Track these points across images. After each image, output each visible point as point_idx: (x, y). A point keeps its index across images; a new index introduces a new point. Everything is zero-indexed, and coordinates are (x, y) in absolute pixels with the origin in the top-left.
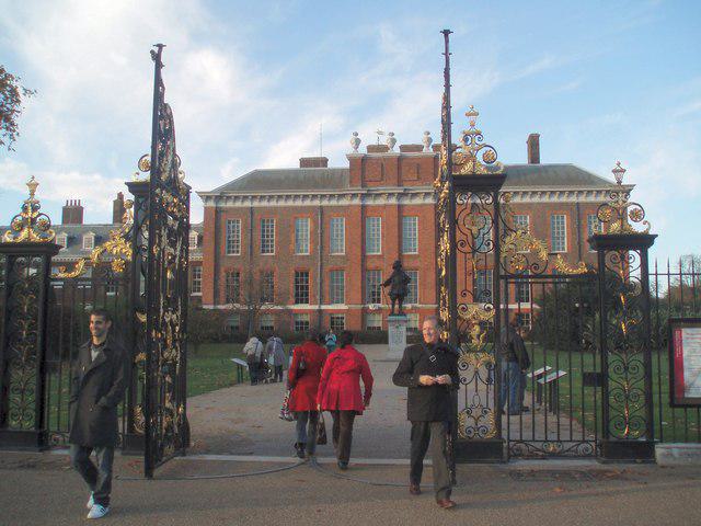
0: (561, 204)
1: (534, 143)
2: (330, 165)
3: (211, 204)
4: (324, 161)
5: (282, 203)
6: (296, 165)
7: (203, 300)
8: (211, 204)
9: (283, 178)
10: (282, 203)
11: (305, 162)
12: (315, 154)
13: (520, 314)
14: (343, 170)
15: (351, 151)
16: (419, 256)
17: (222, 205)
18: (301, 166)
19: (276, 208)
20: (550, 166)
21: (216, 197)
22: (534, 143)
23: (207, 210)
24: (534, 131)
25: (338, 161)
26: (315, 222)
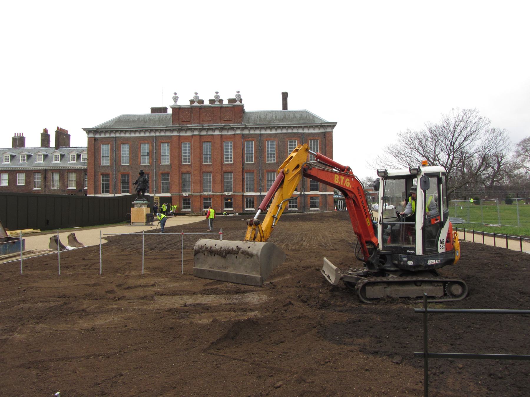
0: (295, 133)
3: (91, 135)
5: (133, 135)
6: (149, 112)
7: (88, 191)
8: (91, 135)
10: (133, 135)
15: (172, 103)
16: (212, 165)
17: (98, 136)
20: (292, 111)
21: (94, 131)
23: (89, 138)
24: (284, 91)
26: (152, 146)
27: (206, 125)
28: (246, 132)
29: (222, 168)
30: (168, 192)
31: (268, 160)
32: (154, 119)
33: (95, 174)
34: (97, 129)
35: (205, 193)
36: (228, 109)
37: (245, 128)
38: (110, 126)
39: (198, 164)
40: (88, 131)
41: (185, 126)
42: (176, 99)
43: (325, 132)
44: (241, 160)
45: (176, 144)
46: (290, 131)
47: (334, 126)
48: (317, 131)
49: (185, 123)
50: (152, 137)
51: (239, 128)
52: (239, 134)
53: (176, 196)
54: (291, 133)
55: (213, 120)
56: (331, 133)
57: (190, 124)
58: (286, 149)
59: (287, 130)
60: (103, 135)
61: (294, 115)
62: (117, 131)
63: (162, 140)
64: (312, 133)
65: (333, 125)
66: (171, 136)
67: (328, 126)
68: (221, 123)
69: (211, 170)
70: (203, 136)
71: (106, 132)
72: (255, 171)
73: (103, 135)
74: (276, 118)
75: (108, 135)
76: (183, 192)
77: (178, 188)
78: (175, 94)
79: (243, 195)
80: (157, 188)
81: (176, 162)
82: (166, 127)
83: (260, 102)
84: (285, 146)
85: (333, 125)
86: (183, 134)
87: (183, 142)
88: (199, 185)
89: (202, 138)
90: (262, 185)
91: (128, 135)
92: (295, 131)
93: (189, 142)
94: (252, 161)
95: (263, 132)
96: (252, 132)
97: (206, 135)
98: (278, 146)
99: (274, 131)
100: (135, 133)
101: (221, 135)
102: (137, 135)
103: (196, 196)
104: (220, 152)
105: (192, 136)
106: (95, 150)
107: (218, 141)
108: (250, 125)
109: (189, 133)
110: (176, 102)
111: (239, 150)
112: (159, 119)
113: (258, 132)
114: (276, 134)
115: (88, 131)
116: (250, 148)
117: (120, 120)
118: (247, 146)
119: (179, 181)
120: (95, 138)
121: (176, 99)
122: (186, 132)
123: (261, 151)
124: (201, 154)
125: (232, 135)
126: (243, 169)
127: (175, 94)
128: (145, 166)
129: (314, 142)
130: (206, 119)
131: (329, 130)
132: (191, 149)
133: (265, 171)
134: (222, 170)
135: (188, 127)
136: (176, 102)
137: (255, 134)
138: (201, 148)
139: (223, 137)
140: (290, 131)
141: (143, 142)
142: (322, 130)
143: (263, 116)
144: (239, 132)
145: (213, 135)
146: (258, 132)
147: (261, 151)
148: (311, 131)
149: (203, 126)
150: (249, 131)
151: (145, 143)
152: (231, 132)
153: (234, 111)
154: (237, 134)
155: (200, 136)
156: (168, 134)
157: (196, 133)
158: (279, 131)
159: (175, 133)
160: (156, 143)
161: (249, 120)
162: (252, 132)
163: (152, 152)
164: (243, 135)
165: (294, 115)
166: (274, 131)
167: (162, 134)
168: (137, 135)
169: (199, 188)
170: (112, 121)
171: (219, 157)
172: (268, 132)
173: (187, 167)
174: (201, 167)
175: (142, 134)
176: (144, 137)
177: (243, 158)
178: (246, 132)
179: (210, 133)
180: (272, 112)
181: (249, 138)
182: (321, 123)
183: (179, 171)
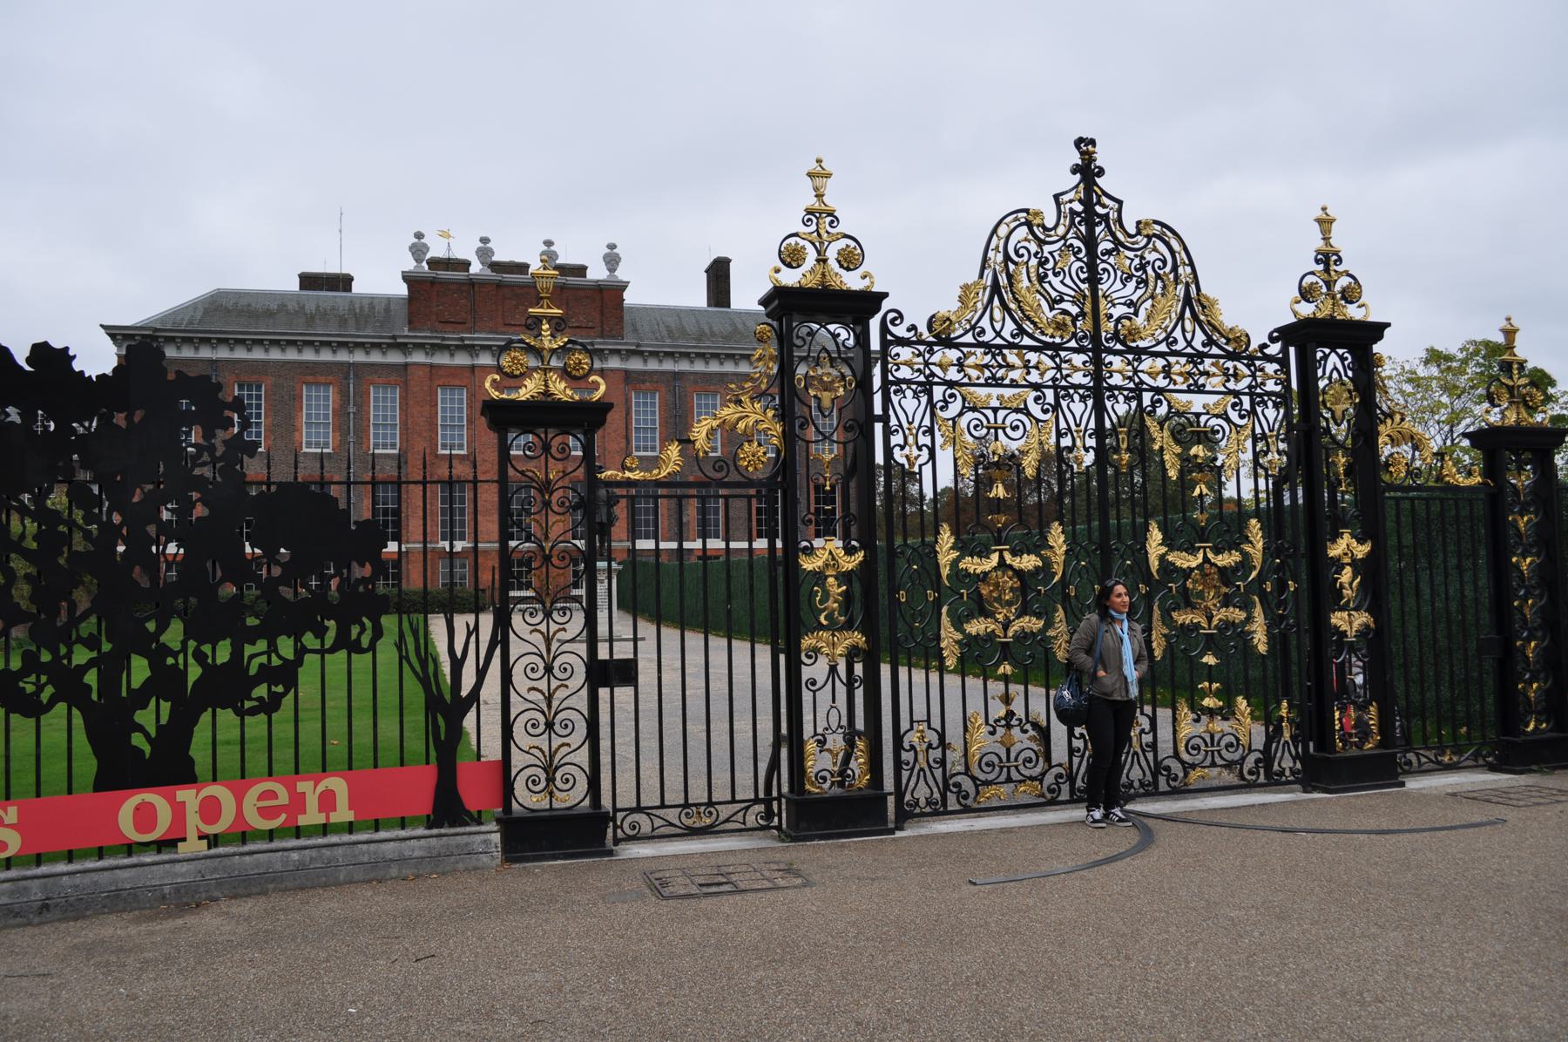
2: (357, 288)
5: (275, 355)
9: (274, 306)
12: (333, 268)
13: (705, 554)
14: (389, 300)
15: (410, 264)
18: (302, 287)
19: (265, 363)
25: (381, 277)
26: (344, 394)
28: (635, 364)
32: (333, 309)
34: (156, 330)
38: (191, 323)
41: (452, 337)
42: (418, 250)
44: (623, 445)
49: (449, 327)
50: (342, 364)
51: (618, 352)
66: (406, 365)
78: (419, 236)
82: (394, 337)
86: (442, 359)
87: (443, 386)
91: (258, 354)
95: (684, 366)
96: (653, 365)
112: (352, 310)
113: (668, 366)
118: (638, 404)
122: (452, 355)
127: (419, 236)
135: (462, 339)
136: (419, 261)
141: (310, 379)
143: (672, 322)
146: (668, 366)
150: (645, 361)
156: (395, 358)
161: (635, 330)
162: (653, 365)
163: (341, 413)
164: (626, 372)
167: (376, 357)
168: (292, 355)
170: (194, 306)
172: (699, 366)
175: (308, 355)
176: (315, 363)
177: (628, 439)
178: (635, 364)
180: (693, 312)
181: (643, 382)
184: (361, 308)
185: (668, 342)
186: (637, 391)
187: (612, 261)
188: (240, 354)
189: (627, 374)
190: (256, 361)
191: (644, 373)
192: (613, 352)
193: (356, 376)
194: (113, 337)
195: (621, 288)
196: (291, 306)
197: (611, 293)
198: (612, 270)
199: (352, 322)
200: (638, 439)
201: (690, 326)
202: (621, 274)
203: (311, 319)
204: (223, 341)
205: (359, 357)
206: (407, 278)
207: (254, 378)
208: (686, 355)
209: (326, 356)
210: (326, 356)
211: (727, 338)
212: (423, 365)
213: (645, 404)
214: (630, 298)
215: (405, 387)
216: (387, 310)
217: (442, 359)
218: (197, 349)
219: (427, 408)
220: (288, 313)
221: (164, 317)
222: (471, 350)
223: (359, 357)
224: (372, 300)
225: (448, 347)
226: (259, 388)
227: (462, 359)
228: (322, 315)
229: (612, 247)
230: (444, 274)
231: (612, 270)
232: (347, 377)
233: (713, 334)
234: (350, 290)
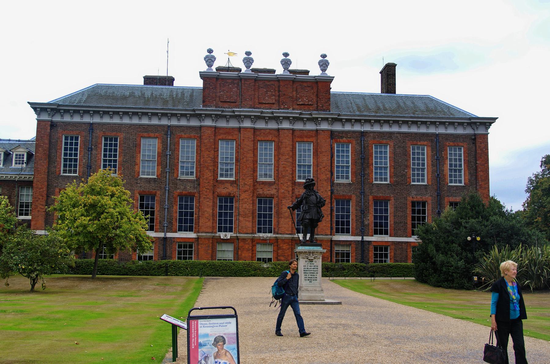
0: (423, 134)
1: (389, 74)
2: (176, 84)
3: (45, 117)
4: (170, 81)
5: (126, 120)
6: (141, 82)
7: (32, 223)
8: (45, 117)
11: (149, 80)
12: (162, 73)
14: (193, 90)
15: (204, 68)
16: (274, 183)
17: (57, 118)
18: (145, 83)
19: (120, 125)
20: (407, 97)
21: (52, 109)
22: (389, 74)
23: (39, 122)
25: (189, 78)
27: (267, 112)
28: (337, 127)
29: (293, 189)
30: (191, 230)
31: (376, 179)
33: (48, 191)
34: (59, 105)
35: (261, 235)
36: (305, 84)
37: (335, 120)
38: (80, 102)
39: (250, 181)
40: (38, 108)
41: (228, 111)
42: (210, 60)
43: (475, 135)
44: (329, 175)
45: (208, 141)
46: (414, 129)
47: (490, 124)
48: (460, 131)
49: (226, 105)
50: (163, 126)
51: (326, 119)
52: (327, 130)
53: (208, 239)
54: (416, 134)
55: (280, 104)
56: (485, 137)
57: (236, 107)
58: (408, 160)
59: (409, 127)
60: (67, 119)
61: (413, 103)
62: (98, 112)
63: (183, 134)
64: (451, 135)
65: (488, 122)
66: (201, 127)
67: (481, 124)
68: (293, 109)
69: (273, 192)
70: (260, 130)
71: (76, 112)
72: (354, 198)
73: (67, 119)
74: (384, 106)
75: (77, 119)
76: (220, 230)
77: (210, 224)
78: (210, 51)
79: (331, 241)
80: (170, 223)
81: (208, 174)
82: (194, 110)
83: (353, 79)
84: (406, 154)
85: (488, 122)
86: (222, 124)
87: (222, 139)
88: (251, 218)
89: (258, 133)
90: (366, 223)
91: (116, 120)
92: (423, 130)
93: (232, 140)
94: (347, 178)
95: (367, 128)
96: (348, 127)
97: (265, 129)
98: (394, 154)
99: (386, 129)
100: (131, 118)
101: (293, 130)
102: (135, 121)
103: (244, 240)
104: (290, 160)
105: (240, 129)
106: (50, 146)
107: (287, 141)
108: (345, 113)
109: (233, 124)
110: (210, 65)
111: (325, 159)
112: (171, 96)
113: (357, 128)
114: (390, 135)
115: (38, 108)
116: (346, 157)
117: (97, 93)
118: (338, 151)
119: (213, 210)
120: (52, 122)
121: (210, 60)
123: (363, 162)
124: (255, 162)
125: (312, 131)
126: (332, 192)
127: (210, 51)
128: (149, 180)
129: (455, 151)
130: (267, 100)
131: (481, 131)
132: (237, 152)
133: (371, 197)
134: (293, 193)
135: (234, 112)
136: (210, 65)
137: (354, 132)
138: (255, 150)
139: (296, 134)
140: (414, 129)
141: (145, 134)
142: (469, 131)
143: (359, 102)
144: (324, 126)
145: (278, 130)
146: (357, 128)
147: (363, 162)
148: (451, 131)
149: (262, 112)
150: (343, 125)
151: (149, 137)
152: (310, 126)
153: (307, 92)
154: (323, 131)
155: (254, 129)
156: (194, 123)
157: (247, 124)
158: (395, 129)
159: (208, 123)
160: (169, 137)
161: (337, 107)
162: (348, 127)
163: (162, 155)
165: (413, 103)
166: (386, 129)
167: (183, 122)
168: (135, 121)
169: (250, 225)
170: (82, 93)
171: (289, 169)
172: (377, 128)
173: (228, 185)
174: (254, 186)
175: (145, 121)
178: (337, 127)
179: (273, 125)
180: (372, 96)
181: (342, 137)
182: (470, 119)
183: (214, 193)
184: (177, 95)
185: (358, 113)
186: (337, 142)
187: (324, 64)
188: (106, 120)
189: (333, 134)
190: (115, 124)
191: (343, 132)
192: (324, 119)
193: (172, 133)
194: (35, 109)
195: (330, 80)
196: (137, 93)
197: (324, 83)
198: (324, 70)
199: (170, 102)
200: (338, 172)
201: (372, 106)
202: (329, 72)
203: (147, 101)
204: (96, 112)
205: (174, 122)
206: (203, 76)
207: (113, 134)
208: (368, 121)
209: (155, 121)
210: (155, 121)
211: (393, 111)
212: (210, 127)
213: (343, 151)
214: (335, 88)
215: (200, 139)
216: (191, 96)
217: (222, 124)
218: (82, 117)
219: (213, 152)
220: (134, 97)
221: (65, 99)
222: (238, 118)
223: (174, 122)
224: (183, 90)
225: (225, 116)
226: (116, 140)
227: (233, 124)
228: (154, 99)
229: (324, 56)
230: (223, 73)
231: (324, 70)
232: (167, 135)
233: (385, 109)
234: (173, 85)
